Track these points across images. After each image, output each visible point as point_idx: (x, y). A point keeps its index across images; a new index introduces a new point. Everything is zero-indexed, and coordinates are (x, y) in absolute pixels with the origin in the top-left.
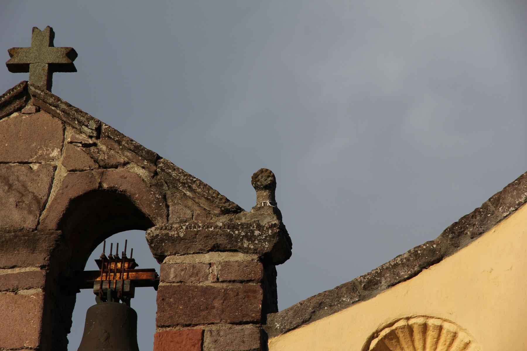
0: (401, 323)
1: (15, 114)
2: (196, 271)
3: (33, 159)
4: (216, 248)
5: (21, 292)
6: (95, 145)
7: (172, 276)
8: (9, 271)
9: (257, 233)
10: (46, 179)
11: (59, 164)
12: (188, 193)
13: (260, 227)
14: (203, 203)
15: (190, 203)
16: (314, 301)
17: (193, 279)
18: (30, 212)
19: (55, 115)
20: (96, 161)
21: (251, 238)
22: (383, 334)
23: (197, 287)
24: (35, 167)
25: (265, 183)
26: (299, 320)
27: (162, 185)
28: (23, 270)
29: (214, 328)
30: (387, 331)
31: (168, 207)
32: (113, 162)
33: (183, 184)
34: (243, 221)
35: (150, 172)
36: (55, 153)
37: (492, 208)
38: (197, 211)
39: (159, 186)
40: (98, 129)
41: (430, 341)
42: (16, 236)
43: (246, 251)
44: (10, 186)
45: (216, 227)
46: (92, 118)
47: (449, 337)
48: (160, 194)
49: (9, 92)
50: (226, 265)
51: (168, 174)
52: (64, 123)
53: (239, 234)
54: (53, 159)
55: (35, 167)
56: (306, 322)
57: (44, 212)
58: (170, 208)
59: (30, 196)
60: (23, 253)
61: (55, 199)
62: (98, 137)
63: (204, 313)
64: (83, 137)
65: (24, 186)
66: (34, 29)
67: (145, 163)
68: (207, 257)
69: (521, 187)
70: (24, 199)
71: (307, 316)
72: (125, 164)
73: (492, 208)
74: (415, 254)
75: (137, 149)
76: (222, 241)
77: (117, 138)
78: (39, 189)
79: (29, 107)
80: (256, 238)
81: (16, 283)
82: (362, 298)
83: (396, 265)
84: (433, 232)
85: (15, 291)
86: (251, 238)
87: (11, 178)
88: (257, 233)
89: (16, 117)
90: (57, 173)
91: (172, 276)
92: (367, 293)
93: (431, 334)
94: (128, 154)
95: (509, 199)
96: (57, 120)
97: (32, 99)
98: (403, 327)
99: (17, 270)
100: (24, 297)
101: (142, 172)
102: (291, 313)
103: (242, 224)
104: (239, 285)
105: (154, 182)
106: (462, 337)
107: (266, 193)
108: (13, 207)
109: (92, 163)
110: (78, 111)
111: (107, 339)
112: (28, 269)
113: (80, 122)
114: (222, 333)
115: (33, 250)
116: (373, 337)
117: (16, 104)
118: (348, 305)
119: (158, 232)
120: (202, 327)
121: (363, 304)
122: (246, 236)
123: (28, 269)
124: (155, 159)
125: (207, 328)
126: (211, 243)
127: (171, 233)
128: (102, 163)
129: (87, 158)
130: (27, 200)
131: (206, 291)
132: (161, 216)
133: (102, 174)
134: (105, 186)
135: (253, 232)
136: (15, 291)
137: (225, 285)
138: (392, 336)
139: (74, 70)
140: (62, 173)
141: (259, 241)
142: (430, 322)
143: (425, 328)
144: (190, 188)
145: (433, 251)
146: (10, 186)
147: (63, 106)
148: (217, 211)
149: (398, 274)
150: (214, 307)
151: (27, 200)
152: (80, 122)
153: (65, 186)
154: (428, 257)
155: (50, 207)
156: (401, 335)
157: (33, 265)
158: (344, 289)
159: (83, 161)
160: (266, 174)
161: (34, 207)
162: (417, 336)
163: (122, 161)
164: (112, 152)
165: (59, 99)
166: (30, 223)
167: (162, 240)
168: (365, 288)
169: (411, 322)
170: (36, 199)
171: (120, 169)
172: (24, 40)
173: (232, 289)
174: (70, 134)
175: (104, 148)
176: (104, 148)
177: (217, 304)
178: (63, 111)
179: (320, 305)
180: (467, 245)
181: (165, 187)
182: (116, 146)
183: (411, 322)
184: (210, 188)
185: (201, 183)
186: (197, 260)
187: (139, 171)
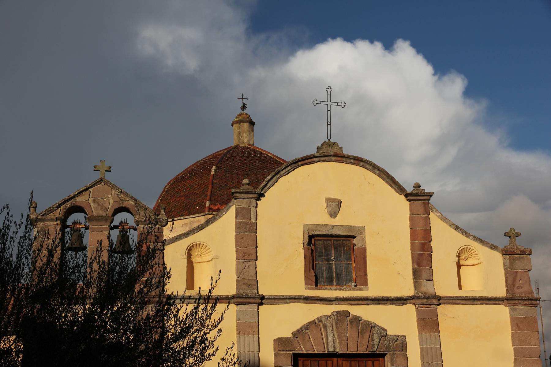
11: (111, 199)
21: (161, 222)
36: (110, 196)
39: (137, 207)
40: (121, 192)
56: (173, 242)
64: (117, 193)
74: (198, 227)
75: (132, 198)
77: (126, 194)
78: (106, 205)
79: (102, 184)
82: (186, 237)
86: (161, 222)
90: (111, 201)
93: (201, 246)
101: (132, 203)
124: (136, 200)
130: (104, 208)
138: (193, 246)
139: (110, 171)
140: (112, 202)
151: (104, 208)
153: (113, 205)
159: (118, 200)
162: (198, 246)
166: (104, 214)
172: (98, 164)
174: (113, 192)
179: (176, 239)
187: (132, 203)
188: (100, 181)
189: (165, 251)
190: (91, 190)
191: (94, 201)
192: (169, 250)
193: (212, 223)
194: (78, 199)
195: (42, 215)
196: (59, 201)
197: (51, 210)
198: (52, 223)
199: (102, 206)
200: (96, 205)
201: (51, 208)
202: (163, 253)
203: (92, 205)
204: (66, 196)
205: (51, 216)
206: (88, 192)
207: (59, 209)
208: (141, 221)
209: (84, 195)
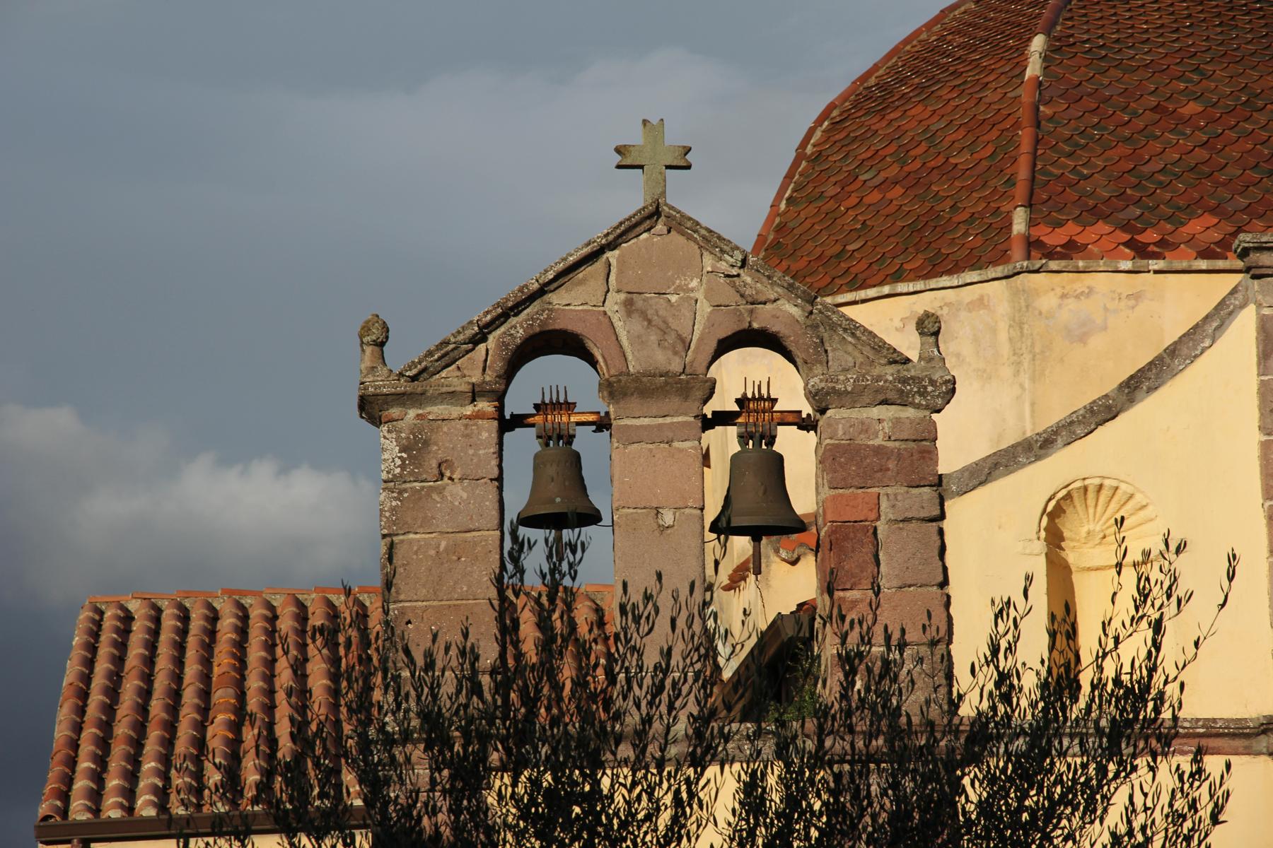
0: (1078, 484)
1: (645, 235)
2: (865, 428)
3: (671, 290)
4: (885, 402)
5: (676, 444)
6: (738, 275)
7: (840, 433)
8: (661, 420)
9: (930, 389)
10: (689, 315)
11: (700, 295)
12: (850, 339)
13: (932, 382)
14: (867, 350)
15: (850, 348)
16: (990, 461)
17: (862, 436)
18: (676, 353)
19: (689, 238)
20: (742, 296)
21: (923, 393)
22: (1060, 495)
23: (868, 446)
24: (674, 298)
25: (932, 330)
26: (976, 482)
27: (817, 327)
28: (675, 420)
29: (889, 490)
30: (1064, 492)
31: (826, 351)
32: (763, 299)
33: (845, 330)
34: (913, 373)
35: (803, 310)
36: (694, 283)
37: (1168, 360)
38: (860, 359)
39: (815, 327)
41: (1103, 498)
42: (666, 383)
43: (918, 406)
44: (650, 321)
45: (886, 381)
46: (738, 248)
47: (1125, 498)
48: (818, 337)
49: (639, 211)
50: (897, 422)
51: (828, 317)
52: (700, 247)
53: (911, 390)
54: (692, 290)
55: (674, 298)
56: (981, 483)
57: (690, 353)
58: (830, 355)
59: (673, 335)
60: (675, 402)
61: (701, 340)
62: (742, 267)
63: (879, 475)
64: (723, 266)
65: (665, 322)
66: (645, 122)
67: (799, 301)
68: (876, 412)
69: (1197, 337)
70: (666, 337)
71: (983, 478)
72: (775, 301)
73: (1168, 360)
74: (1091, 410)
76: (892, 395)
79: (660, 227)
80: (928, 393)
81: (670, 435)
82: (1038, 458)
83: (1072, 423)
84: (1109, 384)
85: (669, 442)
86: (923, 393)
87: (649, 312)
88: (930, 389)
89: (647, 239)
91: (840, 433)
92: (1043, 452)
93: (1105, 494)
94: (779, 290)
95: (1185, 351)
96: (692, 244)
97: (663, 218)
98: (1079, 488)
99: (668, 420)
100: (680, 450)
101: (795, 311)
102: (966, 474)
103: (912, 378)
104: (912, 445)
105: (809, 322)
106: (1139, 498)
107: (932, 339)
108: (656, 346)
109: (738, 298)
110: (719, 237)
111: (765, 493)
112: (680, 419)
113: (722, 251)
114: (899, 498)
115: (686, 398)
116: (1050, 499)
117: (647, 224)
118: (1024, 465)
119: (823, 385)
120: (876, 490)
121: (1039, 463)
122: (918, 392)
123: (680, 419)
125: (882, 491)
126: (880, 397)
127: (838, 387)
128: (750, 299)
129: (733, 291)
130: (671, 338)
131: (878, 451)
132: (821, 362)
133: (751, 312)
134: (755, 325)
135: (925, 387)
136: (669, 442)
137: (897, 444)
138: (1069, 496)
139: (688, 167)
140: (704, 308)
141: (932, 397)
142: (1107, 482)
143: (1101, 487)
144: (853, 335)
145: (1109, 408)
146: (650, 321)
147: (703, 232)
148: (883, 361)
149: (1074, 433)
150: (888, 469)
152: (722, 251)
153: (710, 324)
154: (1103, 412)
155: (697, 347)
156: (1075, 495)
157: (686, 414)
158: (1019, 449)
159: (730, 297)
160: (932, 319)
161: (680, 347)
162: (1091, 495)
163: (772, 297)
164: (759, 285)
165: (698, 224)
167: (828, 393)
168: (1041, 447)
169: (1087, 482)
170: (680, 337)
171: (769, 306)
172: (634, 136)
173: (905, 449)
174: (708, 262)
175: (749, 280)
176: (749, 280)
177: (891, 465)
178: (704, 237)
179: (996, 465)
180: (1142, 400)
181: (821, 329)
182: (765, 279)
183: (1087, 482)
184: (875, 336)
185: (866, 330)
186: (865, 415)
188: (650, 217)
189: (946, 525)
190: (612, 256)
191: (629, 305)
192: (963, 516)
193: (1151, 390)
194: (557, 299)
195: (414, 379)
196: (480, 311)
197: (448, 355)
198: (455, 411)
199: (664, 330)
200: (637, 325)
201: (446, 343)
202: (941, 532)
203: (618, 324)
204: (506, 289)
205: (450, 378)
206: (599, 265)
207: (482, 347)
208: (839, 394)
209: (582, 282)
